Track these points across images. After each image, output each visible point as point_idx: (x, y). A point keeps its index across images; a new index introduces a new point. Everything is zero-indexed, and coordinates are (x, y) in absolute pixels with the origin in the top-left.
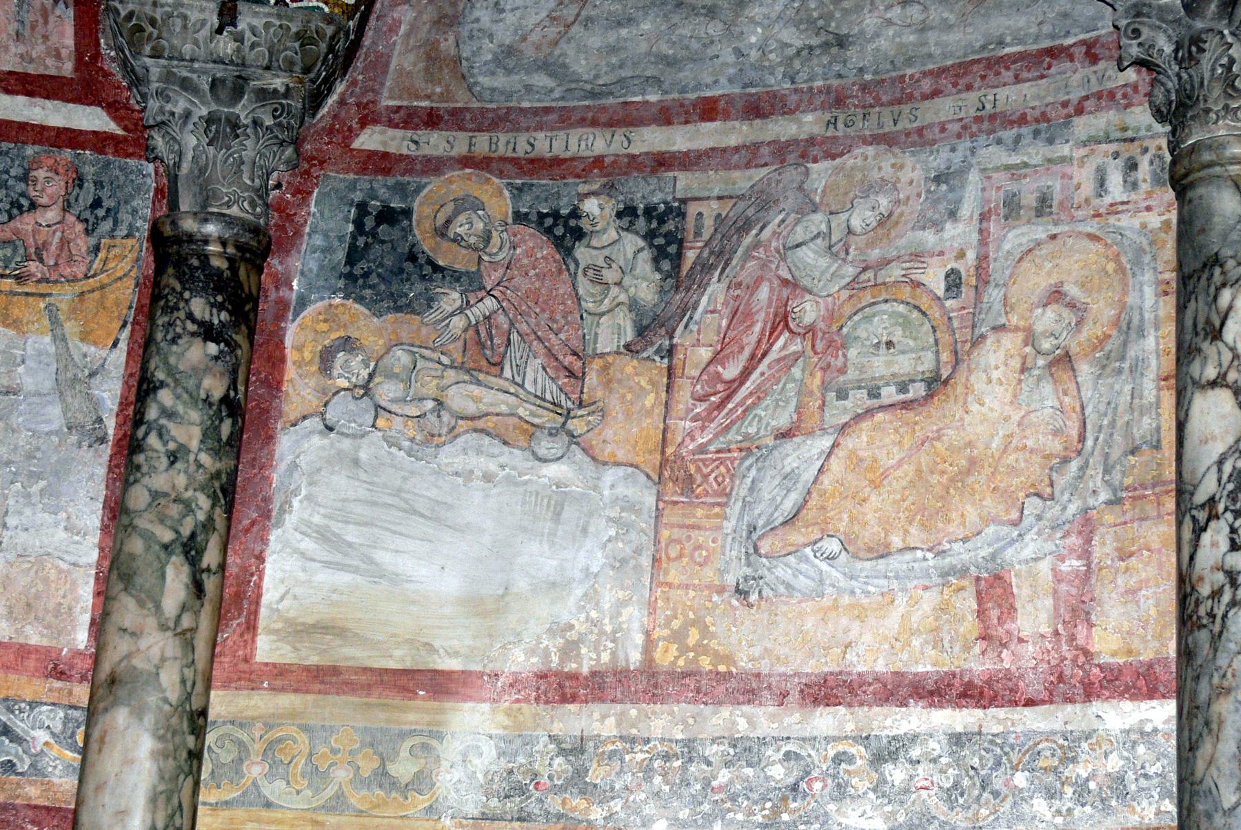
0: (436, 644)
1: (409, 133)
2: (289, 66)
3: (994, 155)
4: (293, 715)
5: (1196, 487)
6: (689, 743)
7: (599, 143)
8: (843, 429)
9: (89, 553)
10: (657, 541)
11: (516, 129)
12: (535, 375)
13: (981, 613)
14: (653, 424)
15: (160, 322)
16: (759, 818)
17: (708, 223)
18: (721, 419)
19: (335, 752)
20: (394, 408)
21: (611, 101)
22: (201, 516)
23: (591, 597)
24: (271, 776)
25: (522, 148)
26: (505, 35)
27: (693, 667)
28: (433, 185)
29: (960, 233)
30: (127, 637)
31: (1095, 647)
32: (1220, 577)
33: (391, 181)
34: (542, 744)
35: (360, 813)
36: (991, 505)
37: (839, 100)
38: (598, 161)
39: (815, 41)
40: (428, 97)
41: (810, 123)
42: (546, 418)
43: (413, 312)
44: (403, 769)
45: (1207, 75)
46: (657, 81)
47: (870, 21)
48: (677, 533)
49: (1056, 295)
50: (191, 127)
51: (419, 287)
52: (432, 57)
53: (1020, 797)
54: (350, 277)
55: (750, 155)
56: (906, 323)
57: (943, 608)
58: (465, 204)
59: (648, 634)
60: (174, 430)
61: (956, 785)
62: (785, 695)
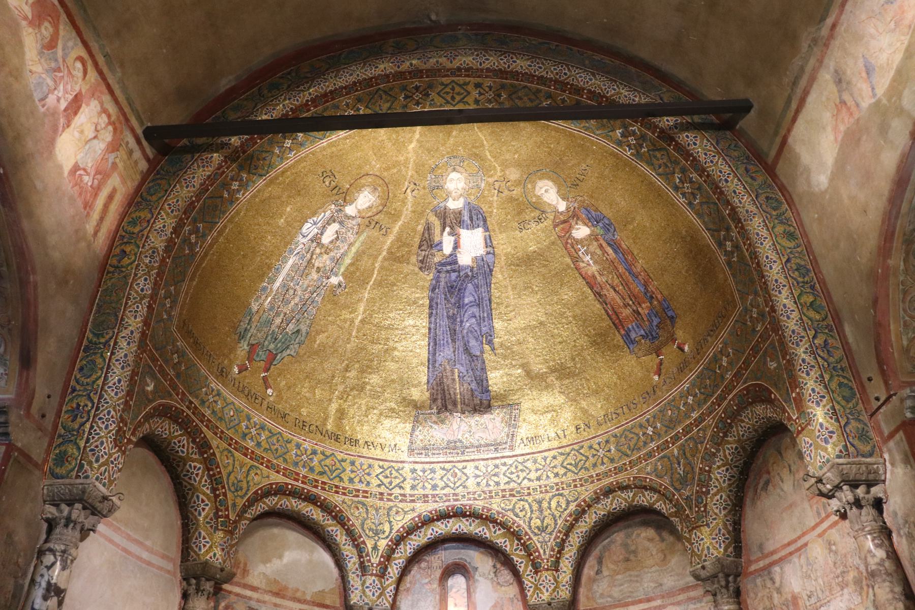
26: (600, 591)
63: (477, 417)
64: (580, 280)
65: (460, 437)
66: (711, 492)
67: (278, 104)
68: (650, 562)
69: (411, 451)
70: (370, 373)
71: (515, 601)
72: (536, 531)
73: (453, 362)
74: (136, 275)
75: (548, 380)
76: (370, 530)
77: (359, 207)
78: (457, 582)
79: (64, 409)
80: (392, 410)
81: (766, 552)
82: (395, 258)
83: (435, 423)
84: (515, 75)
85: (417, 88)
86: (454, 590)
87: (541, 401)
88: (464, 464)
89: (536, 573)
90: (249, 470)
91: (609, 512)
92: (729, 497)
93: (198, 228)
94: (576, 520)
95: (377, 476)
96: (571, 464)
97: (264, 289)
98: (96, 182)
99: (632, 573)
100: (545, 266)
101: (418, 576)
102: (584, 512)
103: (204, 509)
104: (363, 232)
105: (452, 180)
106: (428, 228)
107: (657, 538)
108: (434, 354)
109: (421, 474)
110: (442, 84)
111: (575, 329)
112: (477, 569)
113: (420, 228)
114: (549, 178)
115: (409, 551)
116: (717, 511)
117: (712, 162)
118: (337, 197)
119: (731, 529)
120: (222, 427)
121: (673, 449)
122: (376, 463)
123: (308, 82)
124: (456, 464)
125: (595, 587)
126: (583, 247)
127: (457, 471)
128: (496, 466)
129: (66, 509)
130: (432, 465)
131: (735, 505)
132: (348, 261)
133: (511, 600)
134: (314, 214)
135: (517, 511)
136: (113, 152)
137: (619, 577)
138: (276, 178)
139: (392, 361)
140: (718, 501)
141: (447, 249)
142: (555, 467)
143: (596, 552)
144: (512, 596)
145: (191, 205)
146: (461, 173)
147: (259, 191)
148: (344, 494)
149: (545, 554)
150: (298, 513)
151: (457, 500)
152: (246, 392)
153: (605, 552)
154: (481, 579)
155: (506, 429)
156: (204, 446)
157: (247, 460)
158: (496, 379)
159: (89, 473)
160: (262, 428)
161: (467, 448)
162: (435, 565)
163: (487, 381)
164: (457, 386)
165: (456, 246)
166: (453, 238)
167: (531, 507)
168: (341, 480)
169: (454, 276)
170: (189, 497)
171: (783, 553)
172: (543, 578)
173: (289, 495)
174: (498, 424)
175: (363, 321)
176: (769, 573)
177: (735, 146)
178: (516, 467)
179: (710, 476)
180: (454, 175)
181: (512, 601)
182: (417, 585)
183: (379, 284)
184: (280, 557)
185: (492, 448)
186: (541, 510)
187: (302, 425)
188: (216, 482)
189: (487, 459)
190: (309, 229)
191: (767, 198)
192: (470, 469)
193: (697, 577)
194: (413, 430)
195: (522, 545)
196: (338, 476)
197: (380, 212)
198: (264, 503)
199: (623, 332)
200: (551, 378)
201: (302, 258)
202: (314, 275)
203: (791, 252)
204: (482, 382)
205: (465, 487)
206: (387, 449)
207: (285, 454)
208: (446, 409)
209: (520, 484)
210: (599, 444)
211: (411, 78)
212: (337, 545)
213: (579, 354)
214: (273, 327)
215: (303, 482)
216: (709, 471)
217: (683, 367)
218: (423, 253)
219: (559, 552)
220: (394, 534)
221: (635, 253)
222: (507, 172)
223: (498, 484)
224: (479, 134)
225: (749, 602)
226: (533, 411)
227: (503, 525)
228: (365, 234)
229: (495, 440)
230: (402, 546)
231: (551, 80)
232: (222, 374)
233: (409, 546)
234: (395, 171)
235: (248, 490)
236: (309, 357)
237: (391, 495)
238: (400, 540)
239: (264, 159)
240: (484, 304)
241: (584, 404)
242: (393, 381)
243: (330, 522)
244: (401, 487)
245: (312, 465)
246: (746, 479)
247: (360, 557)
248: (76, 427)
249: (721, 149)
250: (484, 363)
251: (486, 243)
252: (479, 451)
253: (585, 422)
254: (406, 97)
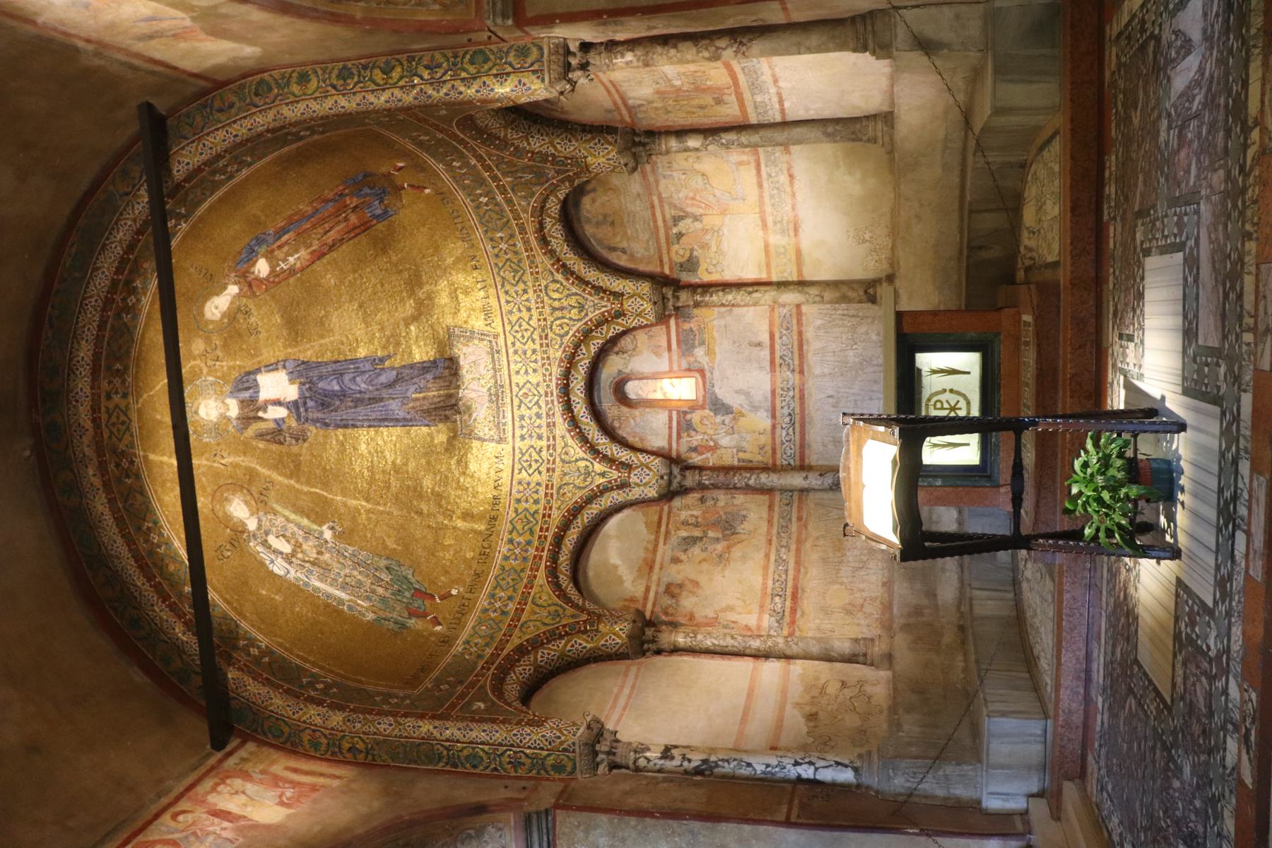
3: (660, 170)
9: (752, 308)
12: (708, 237)
26: (642, 251)
29: (675, 174)
44: (782, 250)
47: (634, 191)
49: (686, 159)
55: (662, 207)
58: (677, 253)
63: (464, 372)
64: (314, 266)
65: (485, 390)
66: (553, 151)
67: (161, 617)
69: (501, 440)
70: (422, 487)
71: (651, 333)
72: (583, 314)
73: (405, 399)
74: (375, 734)
75: (423, 297)
76: (585, 480)
77: (248, 515)
78: (632, 389)
79: (513, 774)
80: (459, 462)
81: (613, 108)
82: (295, 469)
83: (470, 415)
84: (96, 357)
85: (118, 465)
86: (640, 392)
87: (445, 305)
88: (513, 385)
89: (625, 315)
90: (537, 605)
91: (565, 241)
92: (558, 136)
93: (308, 683)
94: (572, 273)
95: (530, 475)
96: (514, 277)
97: (350, 608)
98: (287, 785)
99: (625, 220)
100: (298, 304)
101: (628, 429)
102: (564, 266)
103: (580, 644)
104: (273, 509)
105: (207, 414)
106: (261, 436)
107: (592, 195)
108: (397, 420)
109: (525, 430)
110: (110, 437)
111: (368, 270)
112: (620, 371)
113: (261, 445)
114: (203, 306)
115: (604, 440)
116: (572, 148)
117: (211, 148)
118: (241, 541)
119: (589, 136)
120: (500, 636)
122: (517, 477)
123: (129, 589)
124: (514, 393)
125: (639, 255)
126: (279, 265)
127: (521, 393)
128: (516, 352)
129: (601, 756)
130: (517, 419)
131: (567, 130)
132: (305, 522)
133: (651, 337)
134: (262, 564)
135: (562, 332)
136: (250, 776)
137: (629, 232)
138: (235, 609)
139: (406, 464)
141: (281, 412)
142: (516, 292)
143: (605, 253)
144: (646, 337)
145: (287, 692)
146: (200, 404)
147: (253, 626)
148: (551, 508)
149: (606, 306)
150: (572, 553)
151: (552, 394)
152: (460, 616)
154: (629, 368)
155: (476, 342)
156: (521, 651)
157: (527, 608)
158: (421, 353)
159: (570, 742)
160: (493, 596)
161: (496, 382)
162: (616, 413)
163: (424, 362)
164: (431, 394)
165: (278, 403)
166: (270, 408)
167: (558, 319)
168: (536, 512)
169: (310, 404)
170: (570, 659)
171: (616, 96)
172: (630, 308)
173: (556, 563)
174: (470, 350)
175: (367, 500)
176: (634, 107)
177: (189, 118)
178: (517, 332)
180: (202, 412)
181: (652, 336)
182: (637, 430)
183: (326, 485)
184: (616, 567)
185: (496, 356)
186: (562, 309)
187: (485, 556)
188: (553, 636)
189: (508, 362)
190: (279, 567)
191: (257, 94)
192: (520, 379)
193: (635, 169)
194: (479, 439)
195: (597, 328)
196: (533, 515)
197: (249, 491)
198: (567, 587)
199: (375, 222)
200: (421, 294)
201: (311, 572)
202: (327, 556)
203: (324, 81)
204: (425, 368)
205: (538, 385)
206: (501, 466)
207: (516, 571)
208: (455, 405)
209: (535, 329)
210: (494, 248)
211: (108, 474)
212: (601, 512)
213: (396, 266)
214: (387, 595)
215: (543, 551)
216: (533, 153)
217: (421, 167)
218: (288, 439)
219: (604, 291)
220: (588, 456)
221: (292, 212)
222: (196, 352)
223: (534, 351)
224: (157, 388)
226: (455, 313)
227: (577, 347)
228: (275, 505)
229: (488, 353)
230: (600, 448)
231: (102, 316)
232: (447, 641)
233: (599, 441)
234: (204, 479)
235: (557, 605)
236: (412, 554)
237: (549, 460)
238: (594, 450)
239: (220, 624)
240: (340, 368)
241: (450, 261)
242: (428, 463)
243: (579, 520)
244: (540, 451)
245: (524, 543)
246: (542, 116)
247: (612, 489)
248: (530, 761)
249: (195, 134)
250: (404, 366)
251: (273, 370)
252: (500, 370)
253: (470, 261)
254: (128, 476)
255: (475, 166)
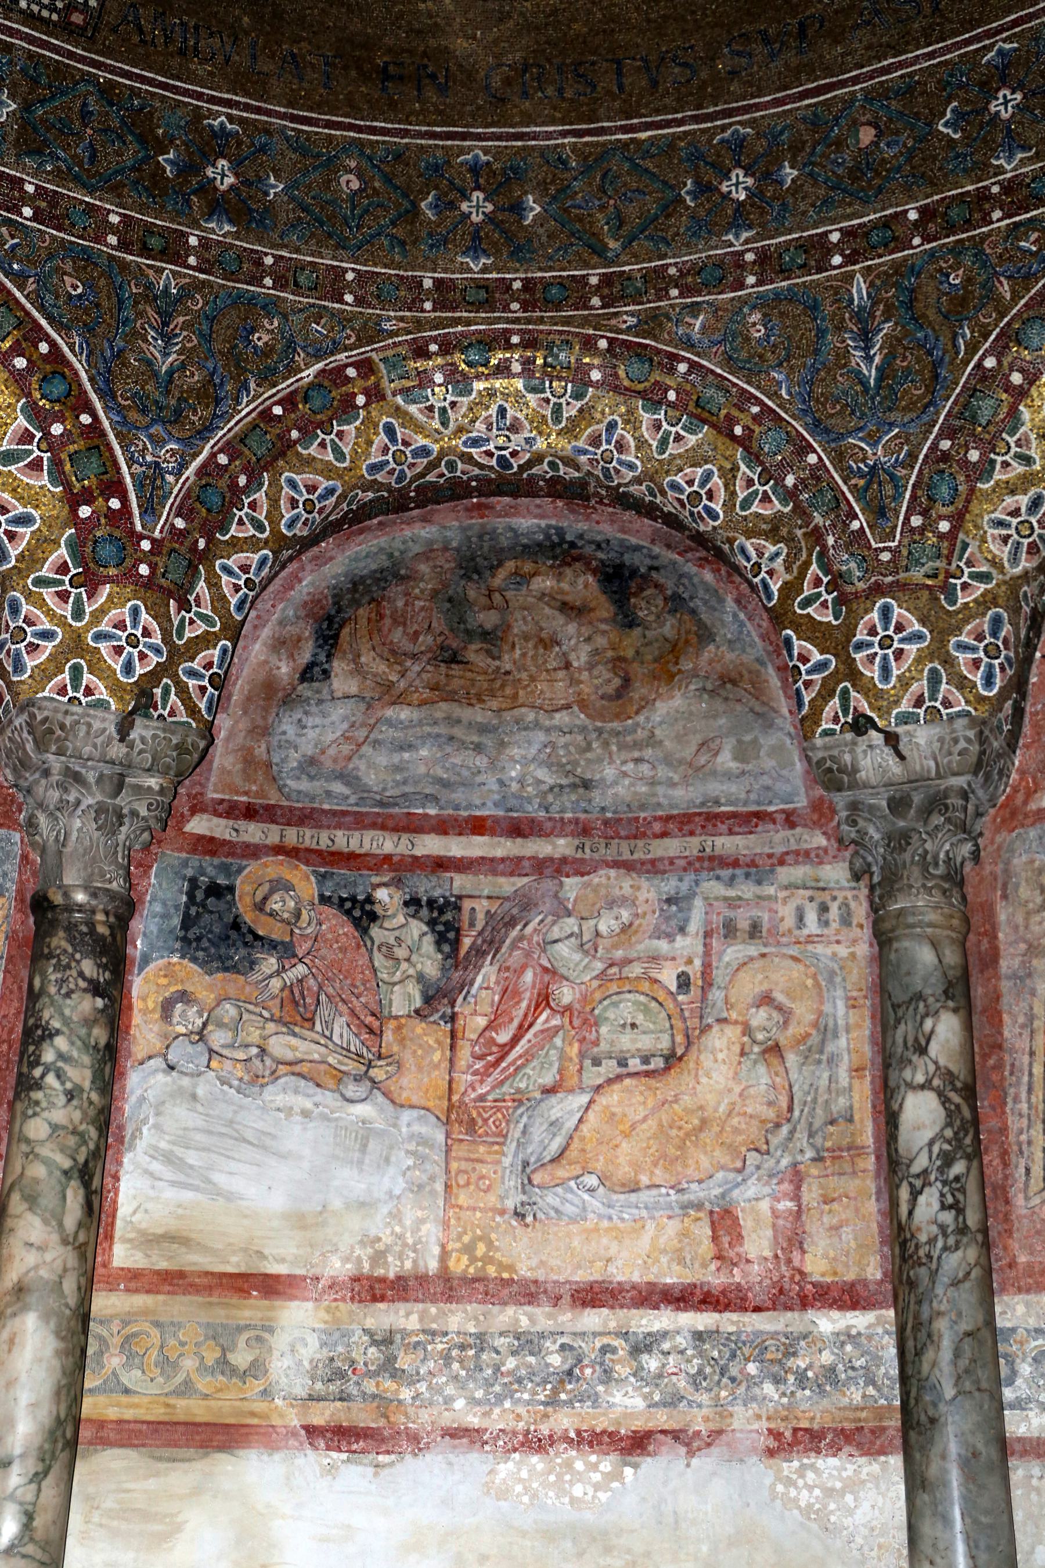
0: (266, 1252)
1: (231, 822)
2: (164, 773)
3: (716, 889)
4: (145, 1312)
5: (911, 1161)
6: (481, 1336)
7: (387, 844)
8: (598, 1088)
10: (448, 1171)
11: (319, 826)
12: (341, 1030)
13: (715, 1238)
14: (440, 1077)
15: (53, 978)
16: (542, 1398)
17: (480, 917)
18: (496, 1074)
19: (183, 1344)
20: (224, 1052)
21: (396, 810)
22: (92, 1146)
23: (396, 1216)
24: (128, 1366)
25: (324, 843)
27: (481, 1274)
28: (252, 867)
29: (689, 944)
30: (34, 1251)
31: (808, 1268)
32: (934, 1229)
33: (216, 861)
34: (358, 1337)
35: (206, 1397)
36: (721, 1156)
37: (585, 831)
38: (388, 858)
39: (564, 782)
40: (246, 793)
41: (561, 846)
42: (350, 1066)
43: (238, 972)
44: (241, 1358)
45: (908, 860)
46: (434, 799)
47: (609, 772)
48: (464, 1165)
49: (766, 1000)
50: (79, 812)
51: (243, 952)
52: (249, 761)
53: (752, 1382)
54: (184, 939)
55: (514, 866)
56: (646, 1010)
57: (684, 1234)
59: (443, 1247)
60: (71, 1072)
61: (700, 1372)
62: (558, 1298)
66: (998, 475)
68: (560, 689)
89: (90, 582)
99: (466, 714)
107: (605, 609)
121: (849, 277)
137: (404, 714)
140: (1015, 513)
153: (356, 603)
179: (1013, 412)
225: (1002, 917)
255: (983, 169)
